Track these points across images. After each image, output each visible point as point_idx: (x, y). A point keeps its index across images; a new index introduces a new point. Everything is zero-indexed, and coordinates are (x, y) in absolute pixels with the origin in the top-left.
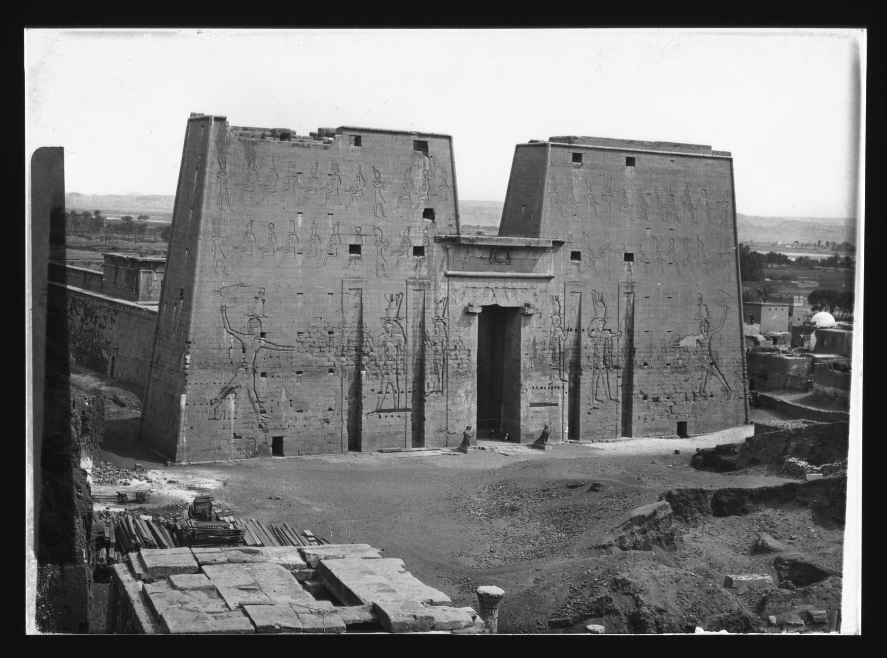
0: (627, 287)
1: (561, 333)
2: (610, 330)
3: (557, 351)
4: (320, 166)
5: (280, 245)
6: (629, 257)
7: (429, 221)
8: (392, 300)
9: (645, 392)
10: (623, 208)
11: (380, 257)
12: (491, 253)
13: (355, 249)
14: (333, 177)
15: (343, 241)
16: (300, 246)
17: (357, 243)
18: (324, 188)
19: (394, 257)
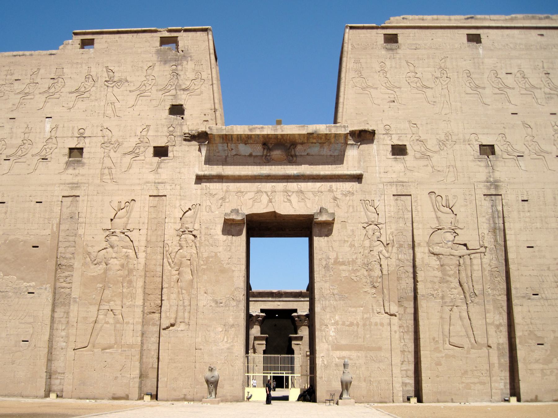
1: (382, 248)
2: (465, 245)
3: (377, 273)
4: (42, 71)
6: (488, 150)
7: (179, 118)
9: (539, 334)
10: (469, 91)
11: (107, 160)
12: (264, 149)
13: (76, 152)
14: (55, 81)
15: (60, 145)
17: (78, 146)
18: (44, 92)
19: (128, 158)
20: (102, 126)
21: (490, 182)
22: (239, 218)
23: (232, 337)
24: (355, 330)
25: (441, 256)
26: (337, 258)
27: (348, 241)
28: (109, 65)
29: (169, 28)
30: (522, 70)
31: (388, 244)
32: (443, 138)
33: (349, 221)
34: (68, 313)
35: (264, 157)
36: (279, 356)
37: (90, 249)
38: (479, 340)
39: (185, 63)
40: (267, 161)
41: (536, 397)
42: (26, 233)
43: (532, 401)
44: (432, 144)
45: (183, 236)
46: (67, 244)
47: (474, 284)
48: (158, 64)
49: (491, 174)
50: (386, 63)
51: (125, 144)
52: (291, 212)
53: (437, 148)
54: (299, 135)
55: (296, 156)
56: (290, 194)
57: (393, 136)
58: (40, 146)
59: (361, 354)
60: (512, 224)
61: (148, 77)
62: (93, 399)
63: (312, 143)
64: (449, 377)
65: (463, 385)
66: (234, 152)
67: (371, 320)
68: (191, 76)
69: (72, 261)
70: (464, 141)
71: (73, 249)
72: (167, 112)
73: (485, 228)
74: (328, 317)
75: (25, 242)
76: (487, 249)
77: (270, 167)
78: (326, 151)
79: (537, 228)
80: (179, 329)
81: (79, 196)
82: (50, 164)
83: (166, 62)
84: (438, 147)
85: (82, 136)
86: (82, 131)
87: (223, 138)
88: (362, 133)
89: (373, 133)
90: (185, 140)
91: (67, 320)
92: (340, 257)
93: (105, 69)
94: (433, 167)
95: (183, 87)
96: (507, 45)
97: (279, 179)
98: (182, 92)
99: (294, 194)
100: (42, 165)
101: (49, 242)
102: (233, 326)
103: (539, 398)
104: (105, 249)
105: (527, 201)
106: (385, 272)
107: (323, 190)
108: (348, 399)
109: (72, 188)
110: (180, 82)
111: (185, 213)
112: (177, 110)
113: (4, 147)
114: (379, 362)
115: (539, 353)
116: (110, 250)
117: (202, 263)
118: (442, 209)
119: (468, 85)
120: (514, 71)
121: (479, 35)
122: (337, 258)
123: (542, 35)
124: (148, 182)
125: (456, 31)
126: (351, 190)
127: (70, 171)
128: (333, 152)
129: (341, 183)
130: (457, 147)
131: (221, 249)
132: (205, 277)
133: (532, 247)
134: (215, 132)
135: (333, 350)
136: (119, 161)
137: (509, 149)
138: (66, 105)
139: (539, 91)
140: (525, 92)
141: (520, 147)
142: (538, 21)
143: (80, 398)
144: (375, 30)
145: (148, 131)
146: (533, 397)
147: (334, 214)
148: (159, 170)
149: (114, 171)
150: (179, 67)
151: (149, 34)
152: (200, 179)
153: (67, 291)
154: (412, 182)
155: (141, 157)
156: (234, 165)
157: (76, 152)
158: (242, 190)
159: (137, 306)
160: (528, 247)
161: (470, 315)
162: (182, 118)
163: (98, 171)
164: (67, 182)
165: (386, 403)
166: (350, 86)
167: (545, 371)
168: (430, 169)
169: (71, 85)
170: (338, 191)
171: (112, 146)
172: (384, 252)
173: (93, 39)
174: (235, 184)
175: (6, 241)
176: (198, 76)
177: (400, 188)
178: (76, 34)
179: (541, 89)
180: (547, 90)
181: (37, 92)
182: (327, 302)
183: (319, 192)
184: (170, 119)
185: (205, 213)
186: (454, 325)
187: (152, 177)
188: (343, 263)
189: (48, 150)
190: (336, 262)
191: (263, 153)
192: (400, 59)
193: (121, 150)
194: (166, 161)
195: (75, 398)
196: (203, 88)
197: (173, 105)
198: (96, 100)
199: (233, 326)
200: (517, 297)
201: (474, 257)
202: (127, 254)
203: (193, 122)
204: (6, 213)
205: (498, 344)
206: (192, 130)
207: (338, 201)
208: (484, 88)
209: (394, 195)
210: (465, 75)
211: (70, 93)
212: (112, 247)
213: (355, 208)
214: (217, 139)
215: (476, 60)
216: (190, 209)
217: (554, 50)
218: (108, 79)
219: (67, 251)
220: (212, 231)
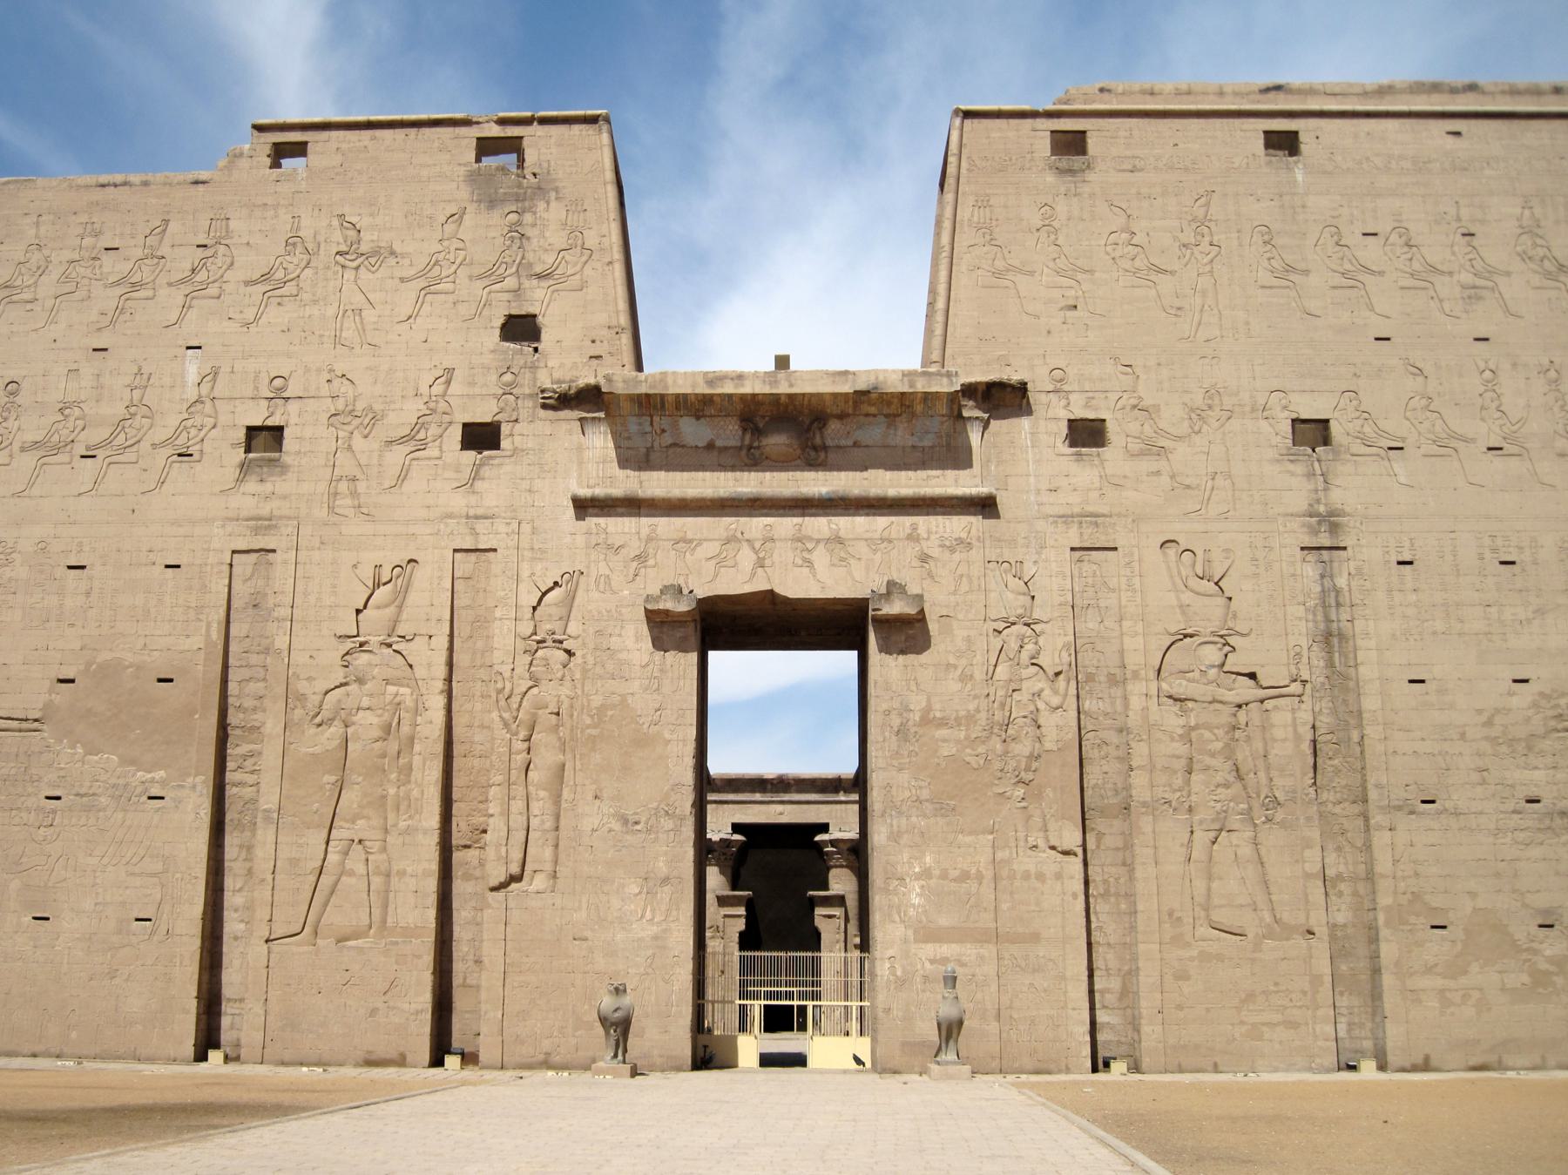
0: (1315, 532)
1: (1041, 684)
2: (1252, 676)
4: (173, 227)
5: (30, 437)
6: (1313, 433)
8: (377, 584)
9: (1436, 901)
10: (1265, 278)
12: (745, 430)
13: (264, 438)
14: (209, 252)
15: (224, 419)
16: (95, 435)
17: (269, 423)
18: (182, 281)
19: (398, 454)
20: (331, 371)
21: (1319, 515)
22: (683, 607)
23: (664, 907)
24: (974, 890)
25: (1190, 704)
26: (929, 709)
27: (955, 667)
28: (346, 210)
29: (502, 114)
30: (1404, 224)
31: (1058, 674)
32: (1198, 399)
33: (960, 616)
34: (250, 848)
35: (744, 452)
36: (783, 954)
37: (302, 686)
38: (1285, 916)
39: (541, 205)
40: (753, 460)
41: (1427, 1058)
42: (140, 645)
43: (1414, 1069)
44: (1172, 416)
45: (540, 653)
46: (246, 673)
47: (1274, 773)
48: (471, 208)
49: (1321, 494)
50: (1058, 208)
51: (392, 418)
52: (814, 592)
53: (1184, 428)
54: (835, 395)
55: (825, 448)
56: (810, 546)
57: (1072, 397)
58: (173, 421)
59: (989, 951)
60: (1371, 623)
61: (446, 243)
62: (316, 1065)
63: (867, 415)
64: (1208, 1010)
65: (1244, 1029)
66: (667, 439)
67: (1015, 867)
68: (557, 238)
69: (259, 716)
70: (1253, 410)
71: (261, 684)
72: (498, 332)
73: (1301, 632)
74: (906, 857)
75: (139, 668)
76: (1308, 686)
77: (760, 474)
78: (901, 436)
79: (1435, 633)
80: (532, 888)
81: (274, 551)
82: (198, 467)
83: (492, 203)
84: (1186, 424)
85: (280, 396)
86: (278, 382)
87: (640, 405)
88: (994, 391)
89: (1021, 389)
90: (544, 406)
91: (248, 865)
92: (937, 706)
93: (335, 222)
94: (1172, 477)
95: (538, 269)
96: (1367, 159)
97: (784, 507)
98: (535, 282)
99: (821, 546)
100: (179, 469)
101: (200, 668)
102: (666, 880)
103: (1434, 1063)
104: (342, 685)
105: (1410, 563)
106: (1049, 745)
107: (894, 536)
108: (954, 1063)
109: (256, 531)
110: (530, 256)
111: (544, 594)
112: (521, 329)
113: (80, 423)
114: (1034, 971)
115: (1436, 948)
116: (353, 688)
117: (588, 721)
118: (1194, 583)
119: (1266, 264)
120: (1383, 227)
121: (1296, 133)
122: (929, 709)
123: (1458, 134)
124: (450, 516)
125: (1237, 122)
126: (963, 535)
127: (251, 485)
128: (921, 440)
129: (940, 518)
130: (1235, 424)
131: (635, 686)
132: (597, 758)
133: (1423, 681)
134: (620, 388)
135: (916, 941)
136: (375, 461)
137: (1367, 429)
138: (237, 316)
139: (1447, 279)
140: (1409, 282)
141: (1396, 426)
142: (1446, 97)
143: (283, 1064)
144: (1029, 121)
145: (448, 382)
146: (1419, 1060)
147: (920, 597)
148: (479, 485)
149: (361, 487)
150: (528, 218)
151: (450, 129)
152: (584, 507)
153: (248, 792)
154: (1119, 515)
155: (432, 451)
156: (668, 470)
157: (264, 438)
158: (690, 535)
159: (425, 832)
160: (1411, 681)
161: (1263, 852)
162: (536, 350)
163: (322, 487)
164: (244, 514)
165: (1049, 1073)
166: (964, 268)
167: (1448, 994)
168: (1165, 479)
169: (250, 263)
170: (933, 537)
171: (358, 421)
172: (1047, 692)
173: (306, 143)
174: (673, 519)
175: (89, 664)
176: (576, 242)
177: (1088, 531)
178: (260, 128)
179: (1451, 273)
180: (1467, 278)
181: (162, 280)
182: (904, 821)
183: (883, 540)
184: (505, 352)
185: (596, 595)
186: (1221, 879)
187: (459, 502)
188: (942, 723)
189: (193, 432)
190: (927, 720)
191: (742, 439)
192: (1092, 195)
193: (381, 433)
194: (496, 462)
195: (270, 1063)
196: (588, 271)
197: (510, 317)
198: (315, 302)
199: (666, 880)
200: (1381, 808)
201: (1276, 708)
202: (398, 699)
203: (564, 359)
204: (88, 594)
205: (1333, 927)
206: (559, 382)
207: (932, 563)
208: (1306, 272)
209: (1073, 549)
210: (1257, 239)
211: (247, 283)
212: (360, 681)
213: (976, 582)
214: (625, 405)
215: (1286, 198)
216: (556, 583)
217: (1488, 172)
218: (344, 248)
219: (247, 691)
220: (614, 639)
